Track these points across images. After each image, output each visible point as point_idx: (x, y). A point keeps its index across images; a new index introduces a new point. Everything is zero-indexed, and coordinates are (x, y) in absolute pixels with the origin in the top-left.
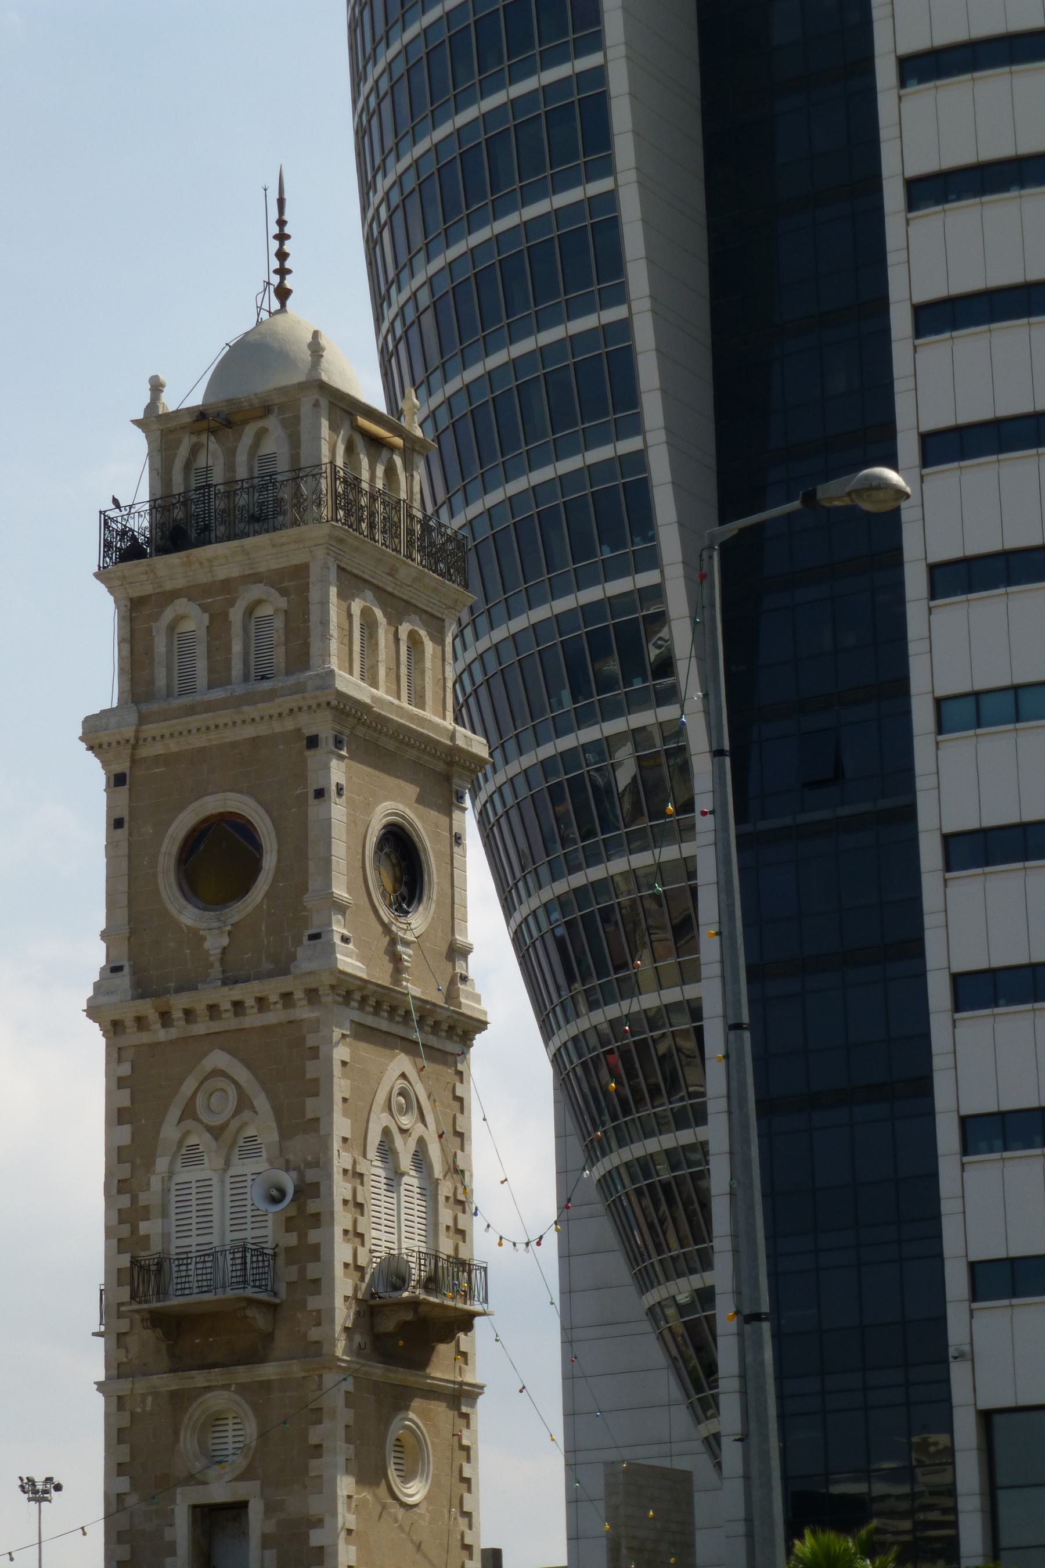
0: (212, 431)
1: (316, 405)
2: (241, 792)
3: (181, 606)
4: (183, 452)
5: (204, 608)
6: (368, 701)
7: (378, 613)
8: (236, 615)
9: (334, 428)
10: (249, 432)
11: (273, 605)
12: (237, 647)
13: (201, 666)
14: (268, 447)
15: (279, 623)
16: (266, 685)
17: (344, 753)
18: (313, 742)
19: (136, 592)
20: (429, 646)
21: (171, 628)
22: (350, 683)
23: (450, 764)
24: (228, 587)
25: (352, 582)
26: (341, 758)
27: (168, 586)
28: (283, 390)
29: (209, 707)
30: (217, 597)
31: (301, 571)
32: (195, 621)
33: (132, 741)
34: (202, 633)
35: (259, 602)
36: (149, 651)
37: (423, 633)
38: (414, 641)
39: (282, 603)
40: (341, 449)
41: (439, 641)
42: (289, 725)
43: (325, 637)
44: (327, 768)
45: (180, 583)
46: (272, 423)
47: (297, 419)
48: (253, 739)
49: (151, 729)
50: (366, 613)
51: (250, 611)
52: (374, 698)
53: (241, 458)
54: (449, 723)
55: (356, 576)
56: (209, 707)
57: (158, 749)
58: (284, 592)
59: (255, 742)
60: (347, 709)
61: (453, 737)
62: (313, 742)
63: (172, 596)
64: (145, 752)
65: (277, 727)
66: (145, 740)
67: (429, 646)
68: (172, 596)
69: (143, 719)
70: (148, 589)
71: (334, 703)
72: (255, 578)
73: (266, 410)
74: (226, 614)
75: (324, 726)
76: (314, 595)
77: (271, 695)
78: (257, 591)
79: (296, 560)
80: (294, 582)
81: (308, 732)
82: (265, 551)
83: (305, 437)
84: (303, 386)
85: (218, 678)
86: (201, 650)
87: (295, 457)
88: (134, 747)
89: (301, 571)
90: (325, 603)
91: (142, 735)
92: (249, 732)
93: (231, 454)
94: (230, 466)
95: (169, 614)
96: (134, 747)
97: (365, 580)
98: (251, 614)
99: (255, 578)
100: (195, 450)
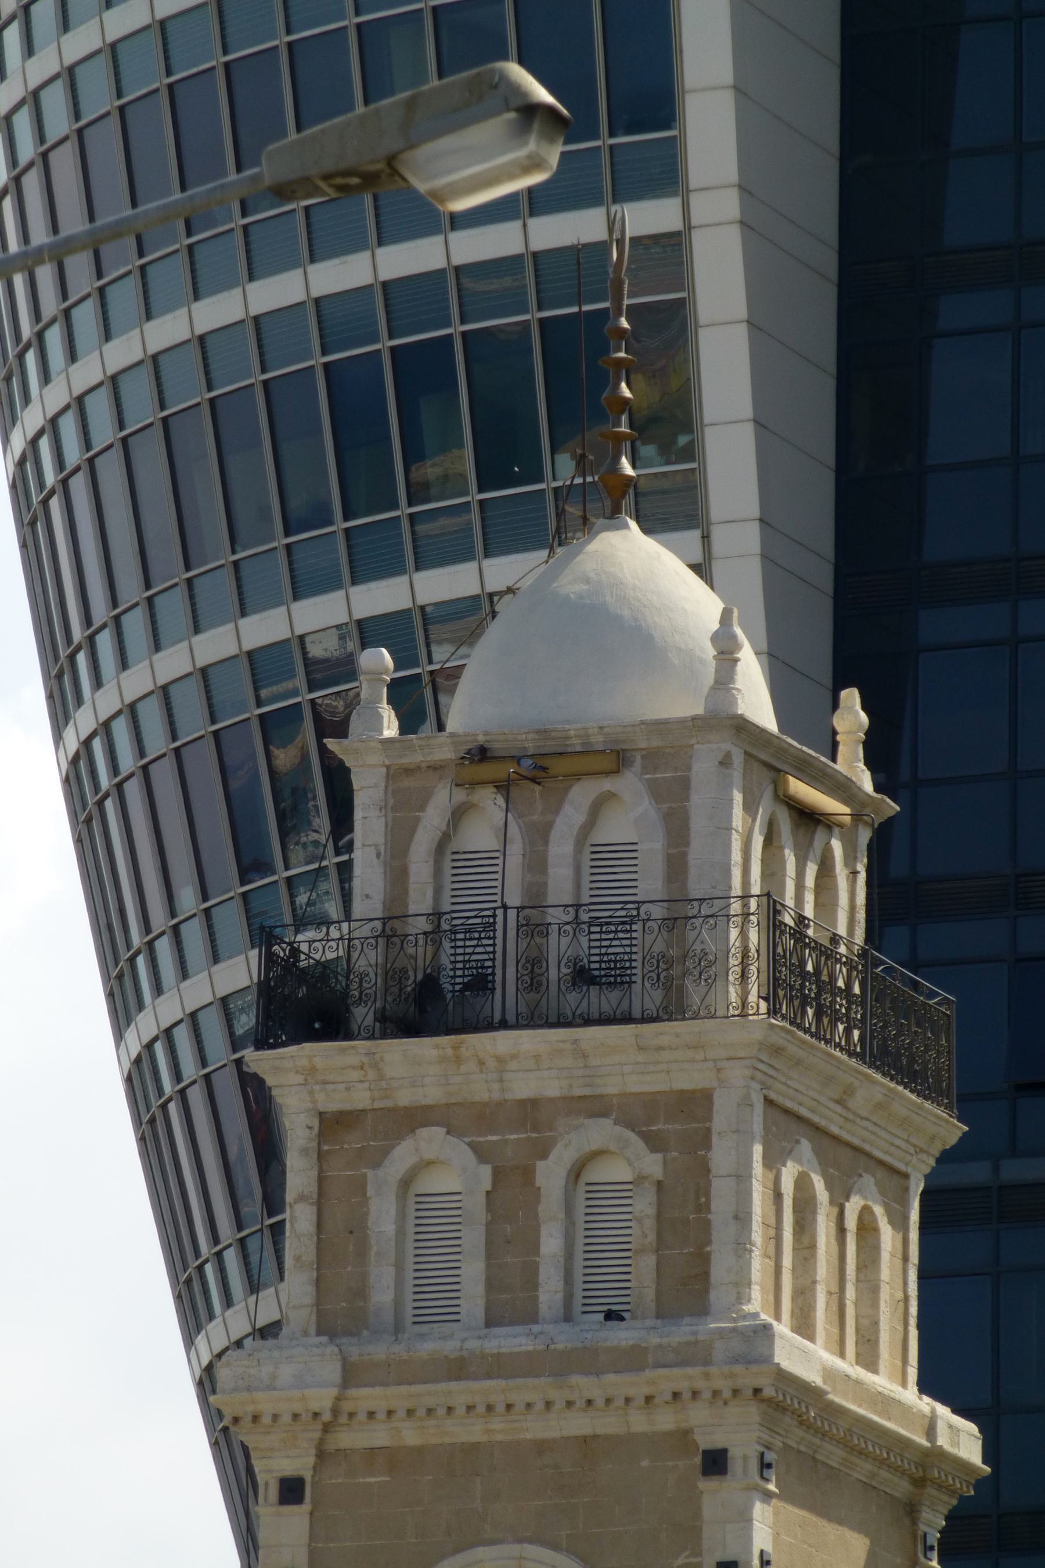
0: (504, 787)
1: (725, 762)
2: (555, 1547)
3: (431, 1140)
4: (433, 819)
5: (481, 1153)
6: (814, 1378)
7: (818, 1183)
8: (551, 1175)
9: (750, 807)
10: (581, 796)
11: (629, 1164)
12: (551, 1243)
13: (472, 1273)
14: (616, 829)
15: (644, 1204)
16: (621, 1335)
17: (772, 1487)
18: (715, 1463)
19: (334, 1102)
20: (887, 1235)
21: (406, 1183)
22: (807, 1357)
23: (919, 1483)
24: (531, 1112)
25: (787, 1124)
26: (768, 1496)
27: (404, 1098)
28: (661, 726)
29: (499, 1367)
30: (512, 1136)
31: (695, 1105)
32: (455, 1173)
33: (327, 1417)
34: (476, 1205)
35: (596, 1155)
36: (358, 1229)
37: (878, 1210)
38: (867, 1228)
39: (653, 1165)
40: (758, 841)
41: (900, 1223)
42: (666, 1421)
43: (742, 1247)
44: (746, 1519)
45: (432, 1094)
46: (629, 785)
47: (685, 784)
48: (585, 1439)
49: (367, 1397)
50: (802, 1183)
51: (576, 1172)
52: (829, 1374)
53: (561, 848)
54: (910, 1395)
55: (787, 1112)
56: (499, 1367)
57: (379, 1436)
58: (654, 1143)
59: (587, 1445)
60: (792, 1404)
61: (931, 1432)
62: (715, 1463)
63: (413, 1119)
64: (346, 1439)
65: (639, 1422)
66: (351, 1415)
67: (887, 1235)
68: (413, 1119)
69: (351, 1375)
70: (361, 1099)
71: (769, 1392)
72: (595, 1107)
73: (616, 758)
74: (528, 1174)
75: (739, 1433)
76: (721, 1157)
77: (634, 1360)
78: (599, 1133)
79: (687, 1080)
80: (678, 1125)
81: (708, 1440)
82: (620, 1058)
83: (699, 824)
84: (699, 725)
85: (510, 1301)
86: (473, 1238)
87: (676, 866)
88: (326, 1428)
89: (695, 1105)
90: (742, 1178)
91: (347, 1406)
92: (579, 1425)
93: (539, 835)
94: (537, 863)
95: (403, 1156)
96: (326, 1428)
97: (799, 1118)
98: (578, 1176)
99: (595, 1107)
100: (458, 814)
